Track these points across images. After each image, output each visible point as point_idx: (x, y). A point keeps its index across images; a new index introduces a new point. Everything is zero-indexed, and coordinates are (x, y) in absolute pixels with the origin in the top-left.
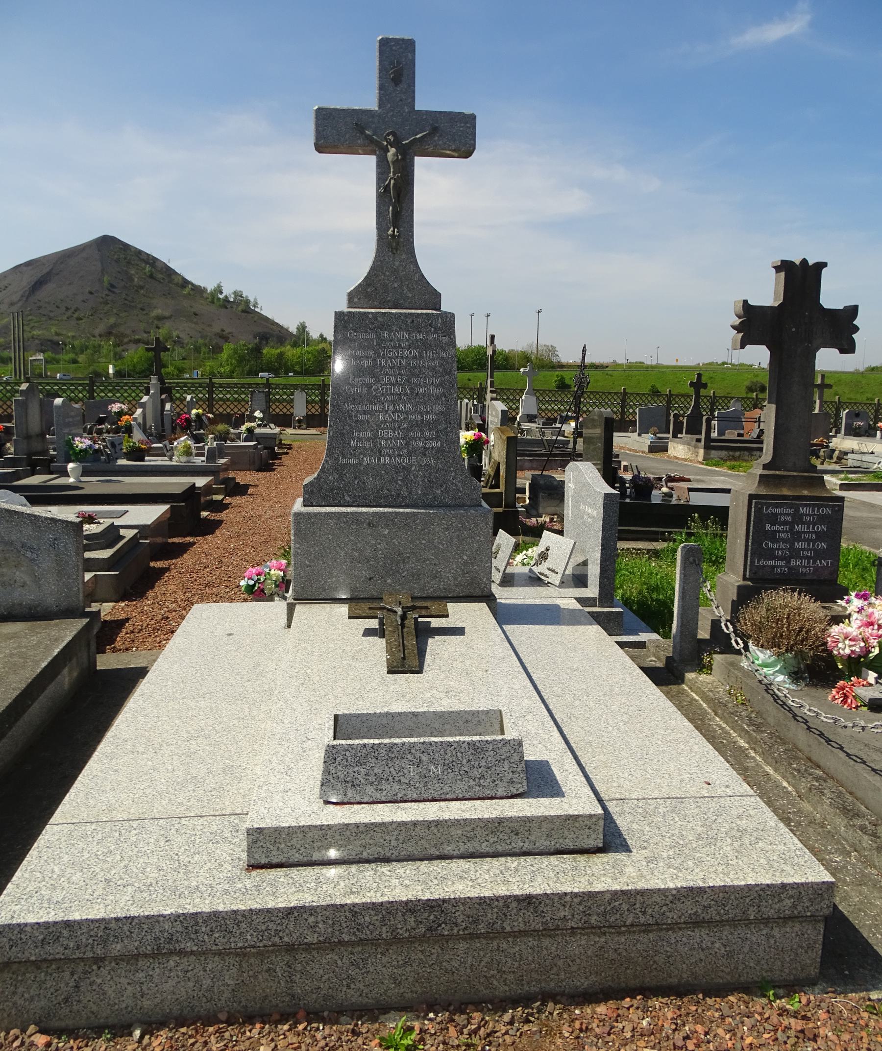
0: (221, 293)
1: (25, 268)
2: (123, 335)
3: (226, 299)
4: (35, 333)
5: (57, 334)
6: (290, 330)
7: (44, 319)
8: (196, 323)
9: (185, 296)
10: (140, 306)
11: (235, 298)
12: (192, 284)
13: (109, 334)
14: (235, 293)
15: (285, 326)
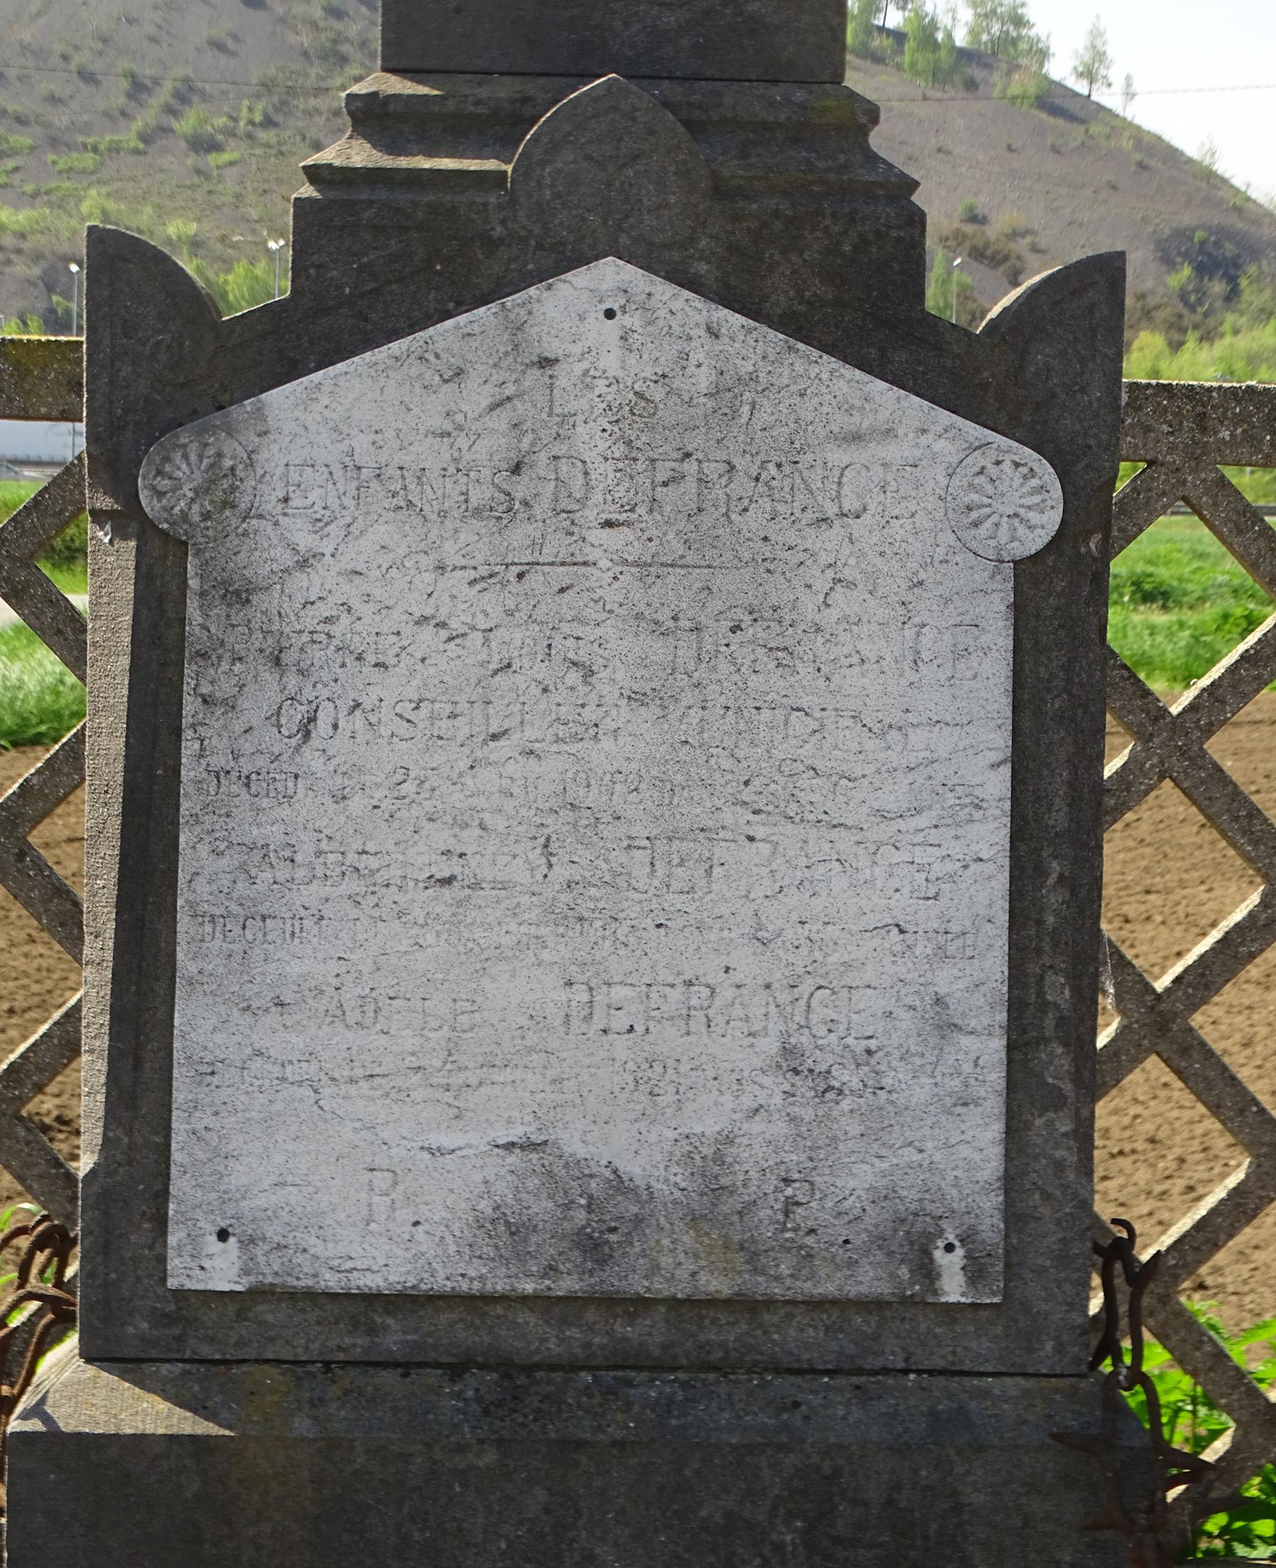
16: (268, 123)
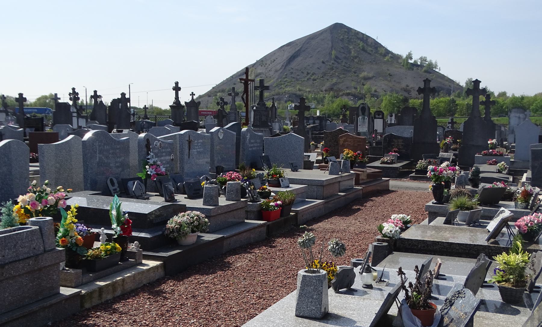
0: (411, 58)
1: (286, 48)
2: (340, 90)
3: (415, 65)
4: (287, 89)
5: (300, 90)
6: (461, 84)
7: (293, 80)
8: (390, 81)
9: (385, 63)
10: (353, 70)
11: (421, 63)
12: (392, 53)
13: (332, 89)
14: (421, 58)
15: (458, 82)
16: (322, 77)
